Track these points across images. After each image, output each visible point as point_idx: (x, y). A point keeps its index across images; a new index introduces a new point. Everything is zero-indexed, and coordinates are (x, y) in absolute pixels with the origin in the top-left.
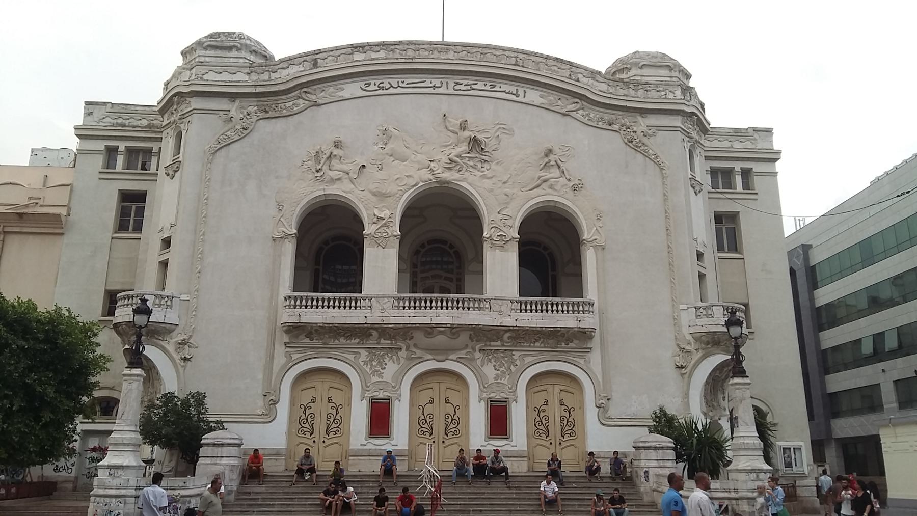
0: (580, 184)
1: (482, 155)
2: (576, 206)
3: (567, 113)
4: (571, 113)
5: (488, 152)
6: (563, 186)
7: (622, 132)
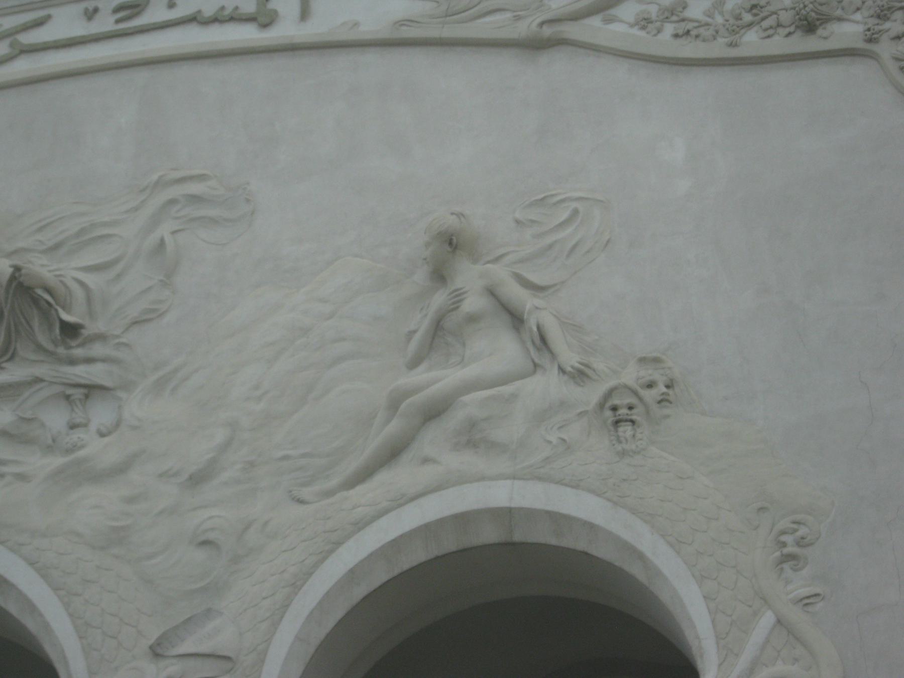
0: (650, 385)
1: (72, 362)
2: (634, 511)
3: (547, 31)
4: (572, 31)
5: (101, 337)
6: (541, 417)
7: (886, 49)
